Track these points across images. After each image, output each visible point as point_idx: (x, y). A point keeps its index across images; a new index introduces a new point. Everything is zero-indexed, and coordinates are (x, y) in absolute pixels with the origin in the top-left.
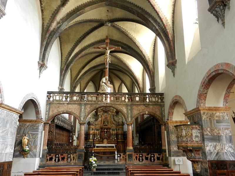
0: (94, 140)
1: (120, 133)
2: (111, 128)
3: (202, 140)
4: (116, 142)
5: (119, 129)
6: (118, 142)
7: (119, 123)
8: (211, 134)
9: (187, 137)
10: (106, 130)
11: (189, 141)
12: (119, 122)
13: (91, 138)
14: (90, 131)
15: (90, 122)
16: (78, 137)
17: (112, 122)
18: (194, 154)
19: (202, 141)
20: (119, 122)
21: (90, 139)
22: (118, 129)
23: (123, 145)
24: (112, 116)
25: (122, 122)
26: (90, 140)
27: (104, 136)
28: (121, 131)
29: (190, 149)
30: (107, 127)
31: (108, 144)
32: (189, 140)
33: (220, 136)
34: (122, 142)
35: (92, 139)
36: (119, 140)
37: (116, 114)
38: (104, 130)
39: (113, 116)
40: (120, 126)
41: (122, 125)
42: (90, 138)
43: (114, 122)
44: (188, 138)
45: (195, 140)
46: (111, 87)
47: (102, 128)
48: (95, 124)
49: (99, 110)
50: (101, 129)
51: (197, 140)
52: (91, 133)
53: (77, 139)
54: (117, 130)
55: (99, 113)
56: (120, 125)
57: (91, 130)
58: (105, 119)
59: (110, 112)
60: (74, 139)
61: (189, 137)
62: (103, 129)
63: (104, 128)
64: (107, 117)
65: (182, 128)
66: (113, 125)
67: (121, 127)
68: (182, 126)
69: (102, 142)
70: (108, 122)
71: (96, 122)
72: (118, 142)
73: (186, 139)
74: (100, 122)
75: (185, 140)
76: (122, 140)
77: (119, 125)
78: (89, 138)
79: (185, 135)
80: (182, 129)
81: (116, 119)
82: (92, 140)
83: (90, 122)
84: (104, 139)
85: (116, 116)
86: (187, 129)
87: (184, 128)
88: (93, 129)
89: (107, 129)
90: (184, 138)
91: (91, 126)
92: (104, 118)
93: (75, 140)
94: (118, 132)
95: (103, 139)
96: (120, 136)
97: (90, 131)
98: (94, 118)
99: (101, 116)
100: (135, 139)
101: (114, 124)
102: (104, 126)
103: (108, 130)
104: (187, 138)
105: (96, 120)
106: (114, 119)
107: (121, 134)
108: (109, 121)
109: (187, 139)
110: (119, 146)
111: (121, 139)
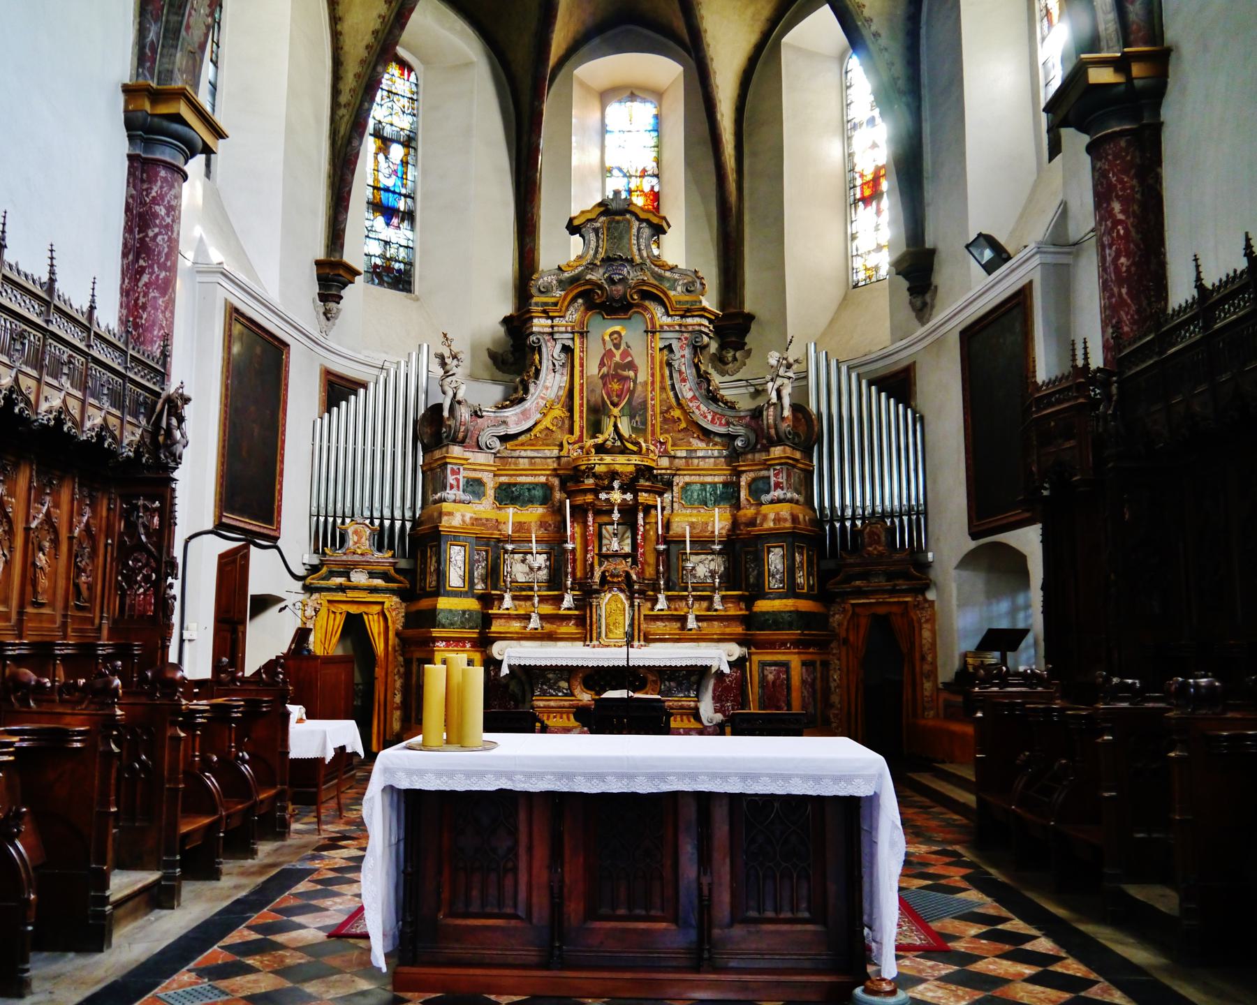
0: (487, 600)
1: (777, 520)
2: (679, 481)
4: (739, 629)
5: (760, 486)
6: (750, 620)
7: (770, 416)
10: (616, 496)
12: (757, 414)
13: (455, 578)
14: (446, 507)
15: (439, 407)
16: (314, 569)
17: (686, 413)
20: (757, 414)
21: (440, 589)
22: (749, 485)
23: (812, 654)
24: (683, 356)
25: (799, 409)
26: (443, 603)
27: (603, 557)
28: (785, 510)
30: (635, 459)
31: (648, 639)
34: (800, 618)
35: (469, 593)
36: (763, 605)
37: (722, 347)
38: (595, 492)
39: (698, 349)
40: (777, 451)
41: (795, 447)
42: (441, 575)
43: (703, 413)
46: (656, 95)
47: (571, 477)
48: (505, 439)
49: (546, 291)
50: (563, 487)
52: (456, 521)
53: (309, 589)
54: (743, 494)
55: (540, 324)
56: (773, 443)
57: (450, 494)
58: (603, 377)
59: (658, 311)
60: (256, 587)
62: (590, 482)
63: (590, 471)
64: (631, 366)
66: (697, 444)
67: (789, 464)
69: (581, 621)
70: (637, 411)
71: (511, 413)
72: (750, 620)
74: (558, 412)
76: (804, 605)
77: (762, 438)
78: (431, 581)
81: (730, 388)
82: (472, 604)
83: (439, 407)
84: (598, 592)
85: (719, 361)
88: (475, 486)
89: (629, 486)
91: (456, 451)
92: (593, 369)
93: (263, 603)
94: (750, 512)
95: (587, 595)
96: (775, 559)
97: (446, 507)
98: (495, 381)
99: (567, 350)
100: (953, 589)
101: (706, 434)
102: (601, 449)
103: (643, 497)
105: (515, 396)
106: (703, 377)
107: (791, 539)
108: (655, 401)
110: (763, 665)
111: (792, 591)
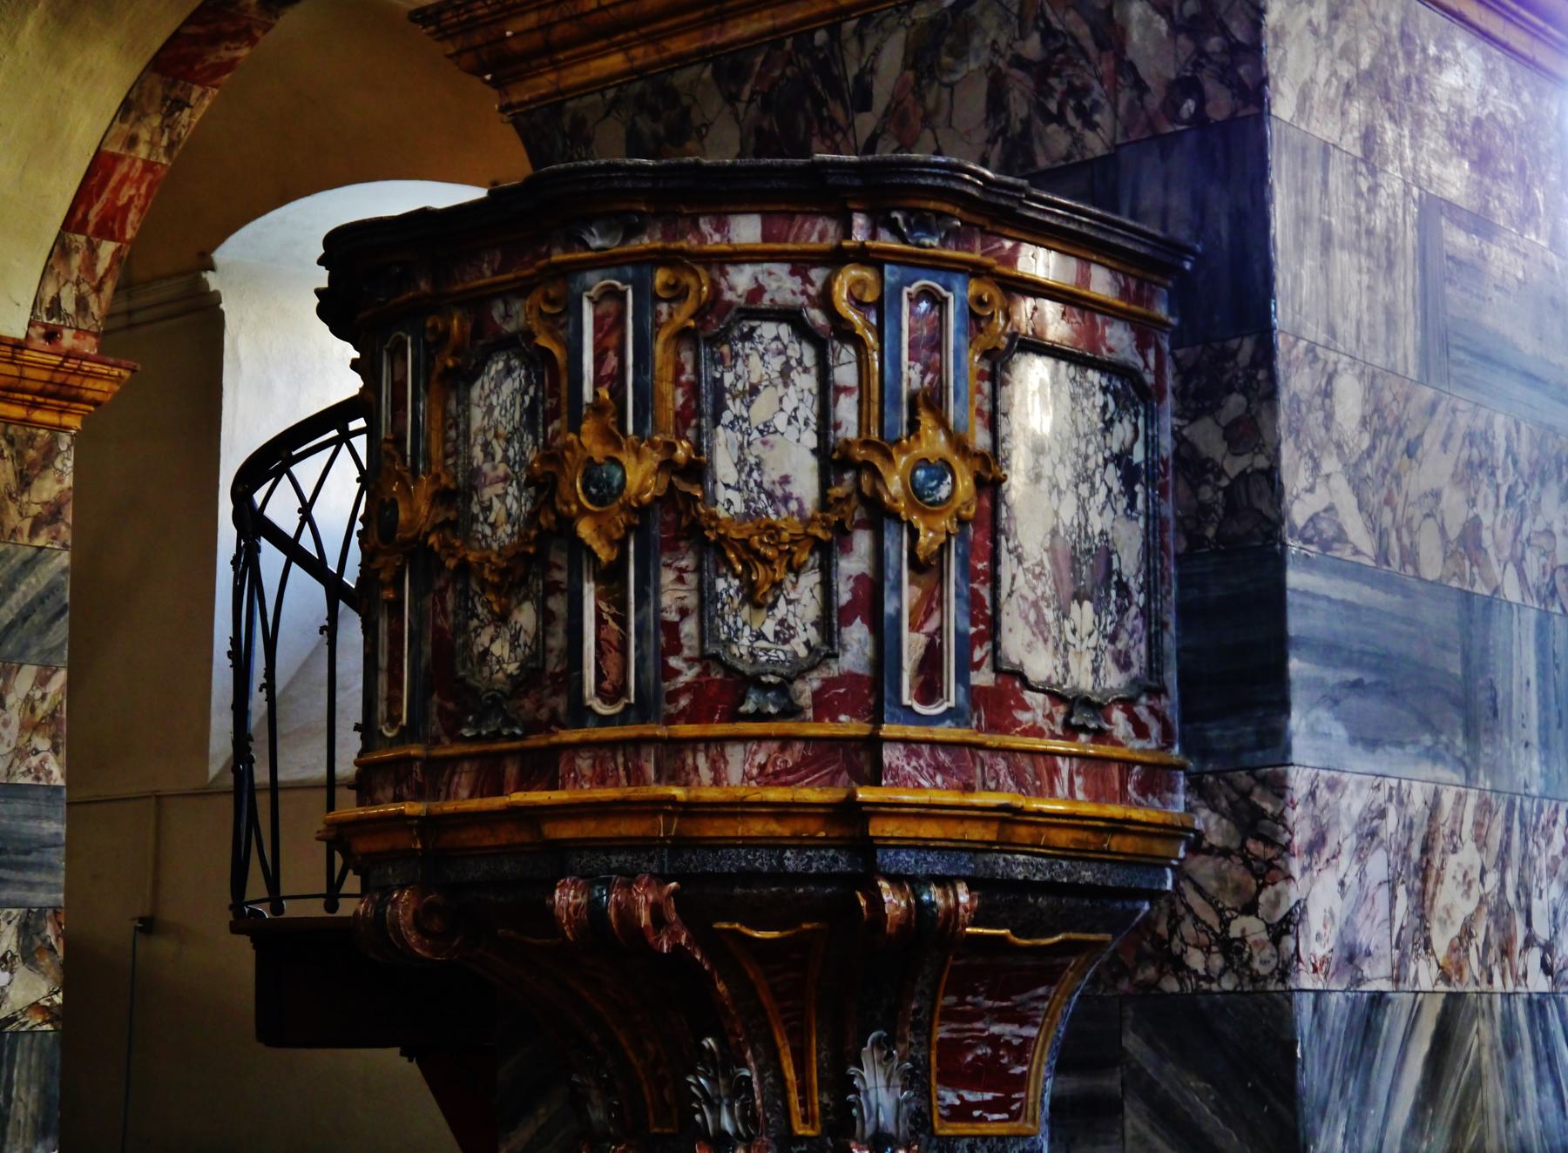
3: (1171, 677)
8: (1383, 556)
9: (854, 563)
11: (929, 689)
18: (915, 1080)
19: (1170, 704)
29: (922, 910)
32: (912, 645)
33: (1489, 603)
44: (906, 596)
45: (1040, 666)
51: (1081, 678)
61: (926, 567)
65: (741, 279)
68: (747, 230)
73: (829, 622)
75: (805, 635)
79: (806, 487)
80: (714, 304)
86: (882, 307)
87: (782, 285)
90: (755, 599)
104: (872, 591)
109: (857, 635)
